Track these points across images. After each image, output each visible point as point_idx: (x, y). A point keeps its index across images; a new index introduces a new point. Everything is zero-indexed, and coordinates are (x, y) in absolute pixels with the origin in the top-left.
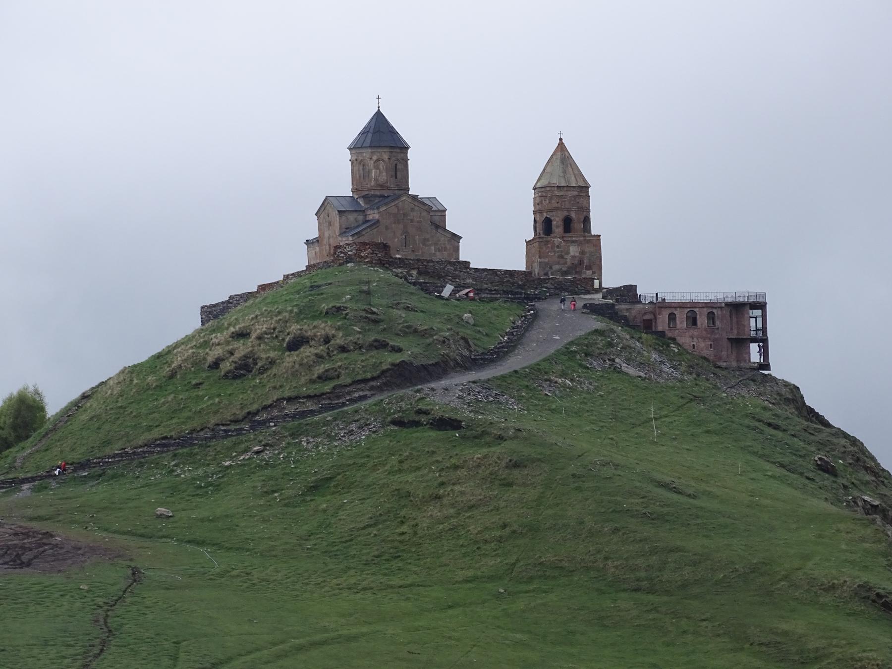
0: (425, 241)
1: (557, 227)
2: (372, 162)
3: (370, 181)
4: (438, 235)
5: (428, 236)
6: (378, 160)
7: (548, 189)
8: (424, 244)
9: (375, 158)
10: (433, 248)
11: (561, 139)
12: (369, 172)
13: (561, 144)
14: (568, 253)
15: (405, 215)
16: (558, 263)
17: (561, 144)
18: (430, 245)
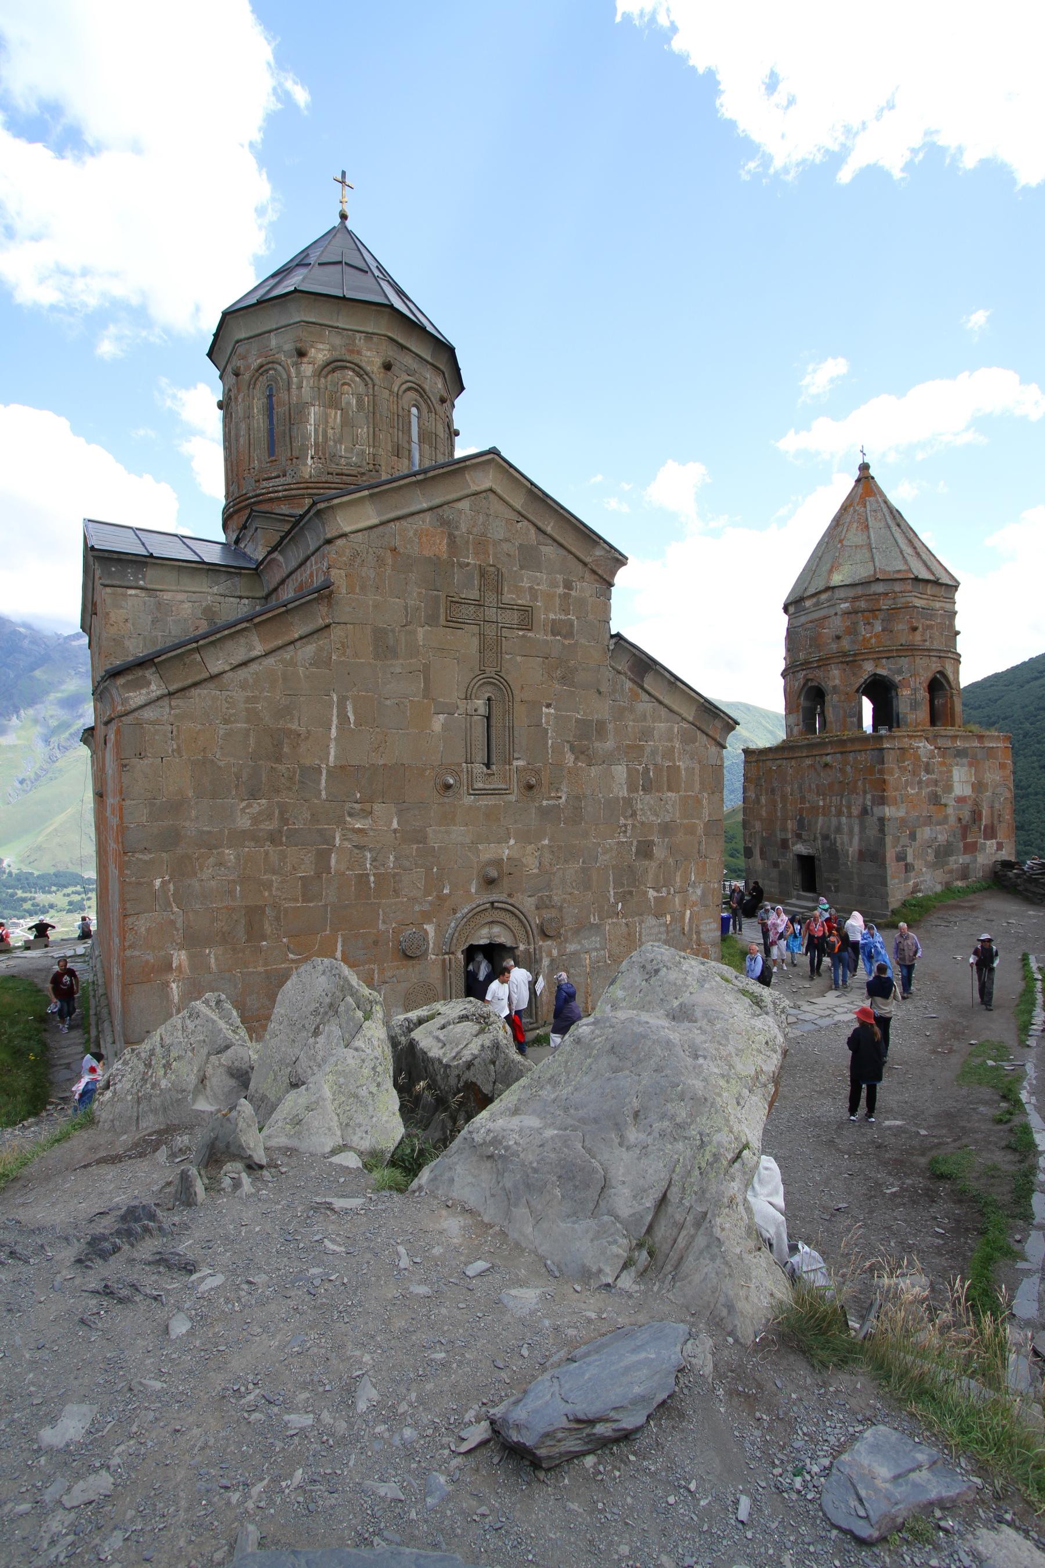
0: (585, 737)
1: (914, 706)
2: (307, 369)
3: (297, 458)
4: (645, 706)
5: (601, 710)
6: (334, 366)
7: (880, 588)
8: (580, 752)
9: (319, 354)
10: (620, 771)
11: (864, 467)
12: (296, 415)
13: (865, 479)
14: (949, 788)
15: (491, 580)
16: (929, 821)
17: (865, 479)
18: (609, 760)
